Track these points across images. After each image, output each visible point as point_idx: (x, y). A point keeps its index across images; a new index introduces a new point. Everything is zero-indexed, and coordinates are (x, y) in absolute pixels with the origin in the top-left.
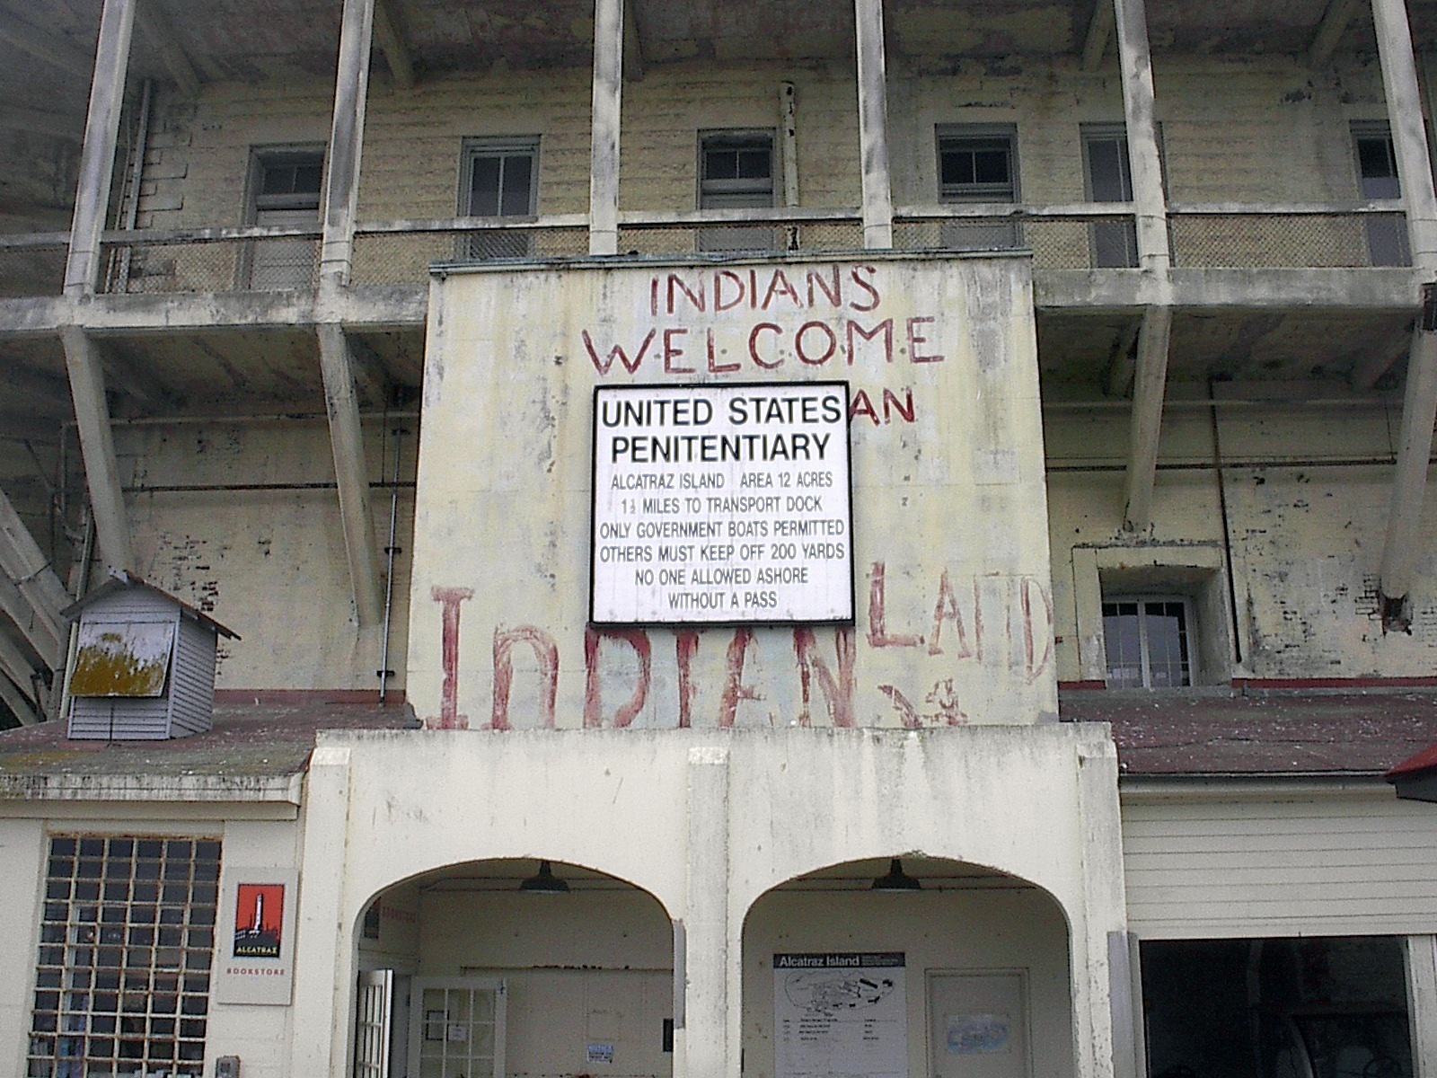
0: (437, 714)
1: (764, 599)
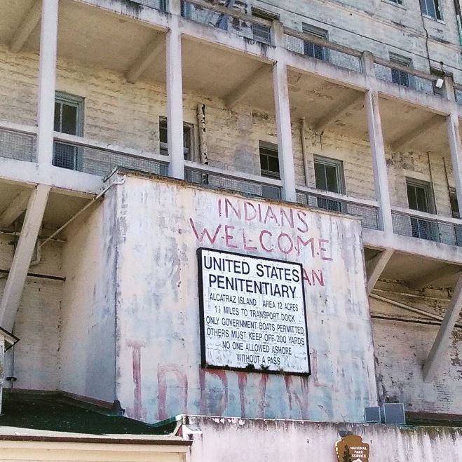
0: (132, 407)
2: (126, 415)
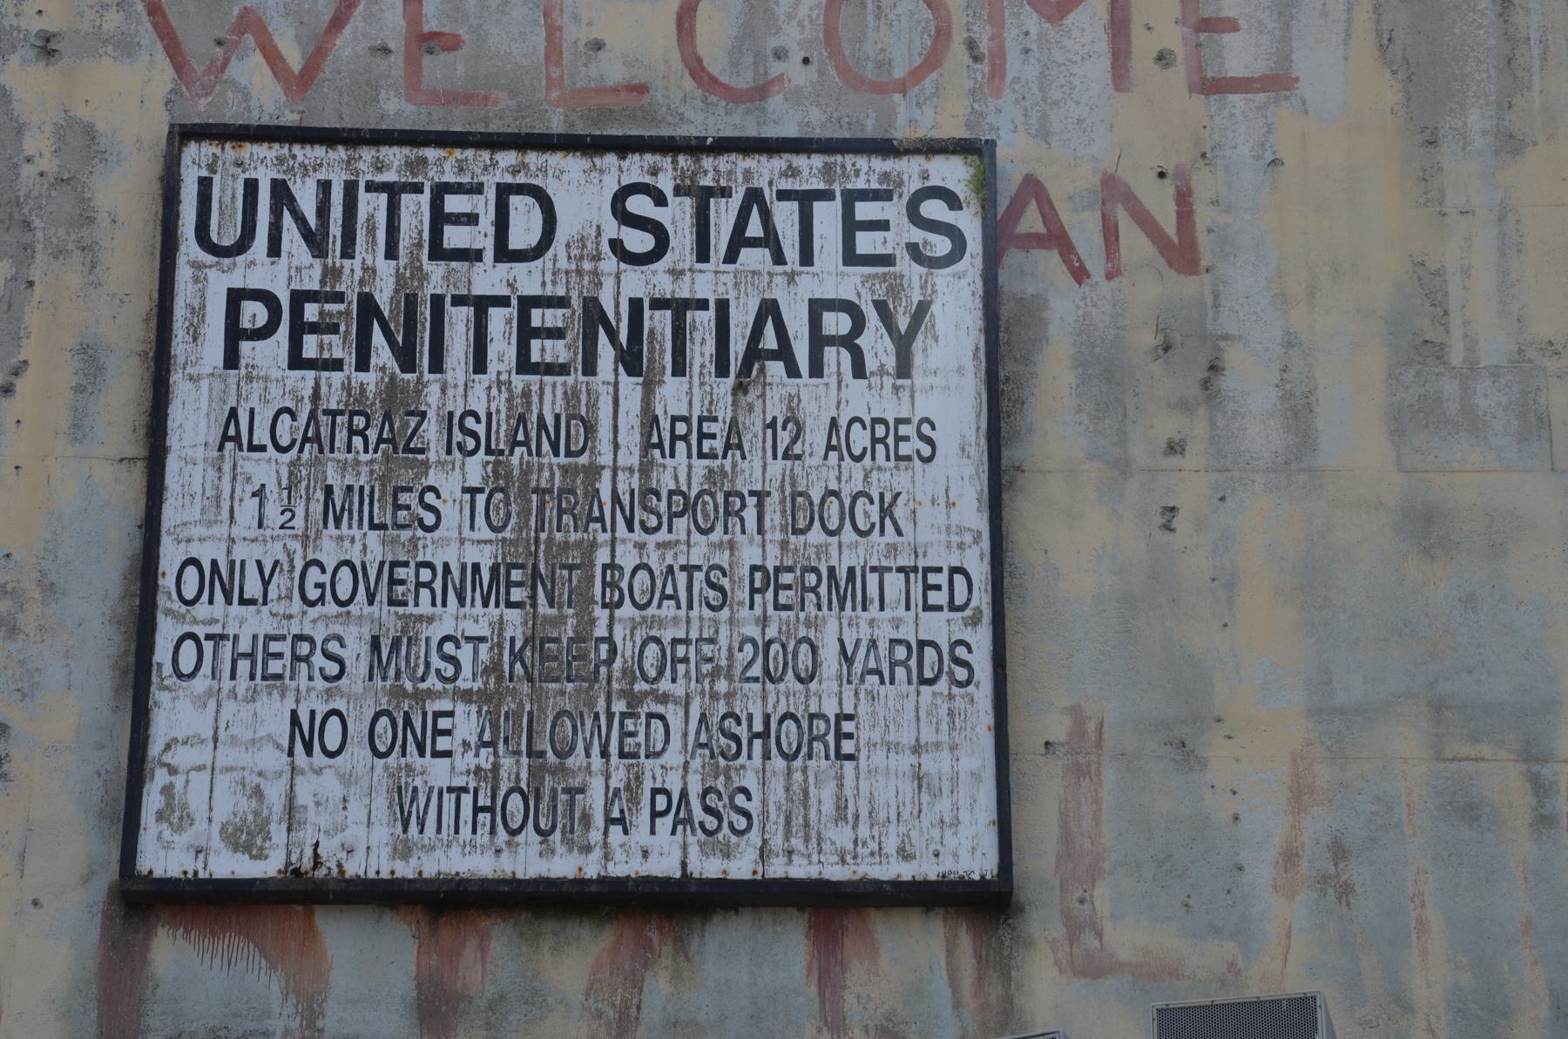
1: (708, 810)
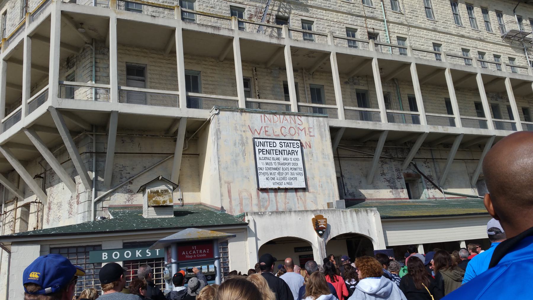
0: (229, 208)
2: (226, 212)
